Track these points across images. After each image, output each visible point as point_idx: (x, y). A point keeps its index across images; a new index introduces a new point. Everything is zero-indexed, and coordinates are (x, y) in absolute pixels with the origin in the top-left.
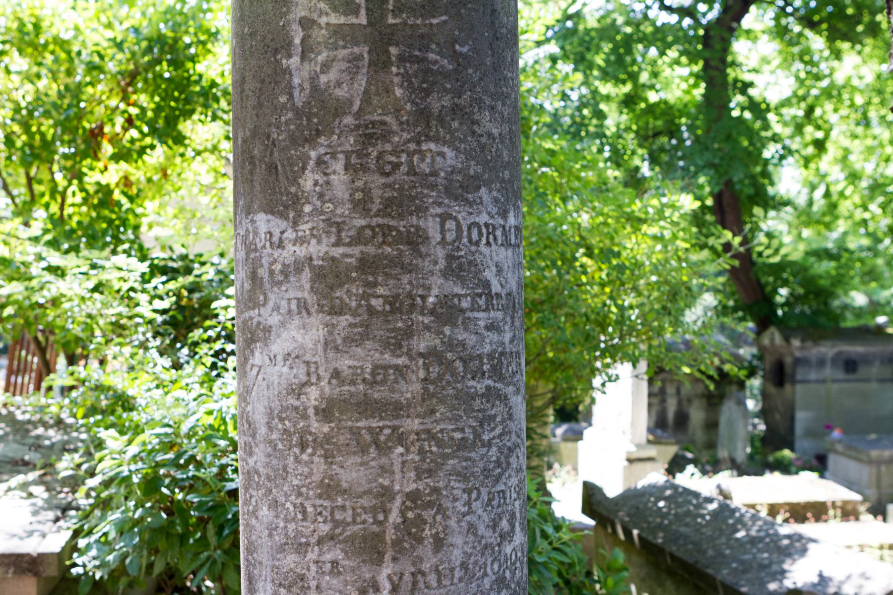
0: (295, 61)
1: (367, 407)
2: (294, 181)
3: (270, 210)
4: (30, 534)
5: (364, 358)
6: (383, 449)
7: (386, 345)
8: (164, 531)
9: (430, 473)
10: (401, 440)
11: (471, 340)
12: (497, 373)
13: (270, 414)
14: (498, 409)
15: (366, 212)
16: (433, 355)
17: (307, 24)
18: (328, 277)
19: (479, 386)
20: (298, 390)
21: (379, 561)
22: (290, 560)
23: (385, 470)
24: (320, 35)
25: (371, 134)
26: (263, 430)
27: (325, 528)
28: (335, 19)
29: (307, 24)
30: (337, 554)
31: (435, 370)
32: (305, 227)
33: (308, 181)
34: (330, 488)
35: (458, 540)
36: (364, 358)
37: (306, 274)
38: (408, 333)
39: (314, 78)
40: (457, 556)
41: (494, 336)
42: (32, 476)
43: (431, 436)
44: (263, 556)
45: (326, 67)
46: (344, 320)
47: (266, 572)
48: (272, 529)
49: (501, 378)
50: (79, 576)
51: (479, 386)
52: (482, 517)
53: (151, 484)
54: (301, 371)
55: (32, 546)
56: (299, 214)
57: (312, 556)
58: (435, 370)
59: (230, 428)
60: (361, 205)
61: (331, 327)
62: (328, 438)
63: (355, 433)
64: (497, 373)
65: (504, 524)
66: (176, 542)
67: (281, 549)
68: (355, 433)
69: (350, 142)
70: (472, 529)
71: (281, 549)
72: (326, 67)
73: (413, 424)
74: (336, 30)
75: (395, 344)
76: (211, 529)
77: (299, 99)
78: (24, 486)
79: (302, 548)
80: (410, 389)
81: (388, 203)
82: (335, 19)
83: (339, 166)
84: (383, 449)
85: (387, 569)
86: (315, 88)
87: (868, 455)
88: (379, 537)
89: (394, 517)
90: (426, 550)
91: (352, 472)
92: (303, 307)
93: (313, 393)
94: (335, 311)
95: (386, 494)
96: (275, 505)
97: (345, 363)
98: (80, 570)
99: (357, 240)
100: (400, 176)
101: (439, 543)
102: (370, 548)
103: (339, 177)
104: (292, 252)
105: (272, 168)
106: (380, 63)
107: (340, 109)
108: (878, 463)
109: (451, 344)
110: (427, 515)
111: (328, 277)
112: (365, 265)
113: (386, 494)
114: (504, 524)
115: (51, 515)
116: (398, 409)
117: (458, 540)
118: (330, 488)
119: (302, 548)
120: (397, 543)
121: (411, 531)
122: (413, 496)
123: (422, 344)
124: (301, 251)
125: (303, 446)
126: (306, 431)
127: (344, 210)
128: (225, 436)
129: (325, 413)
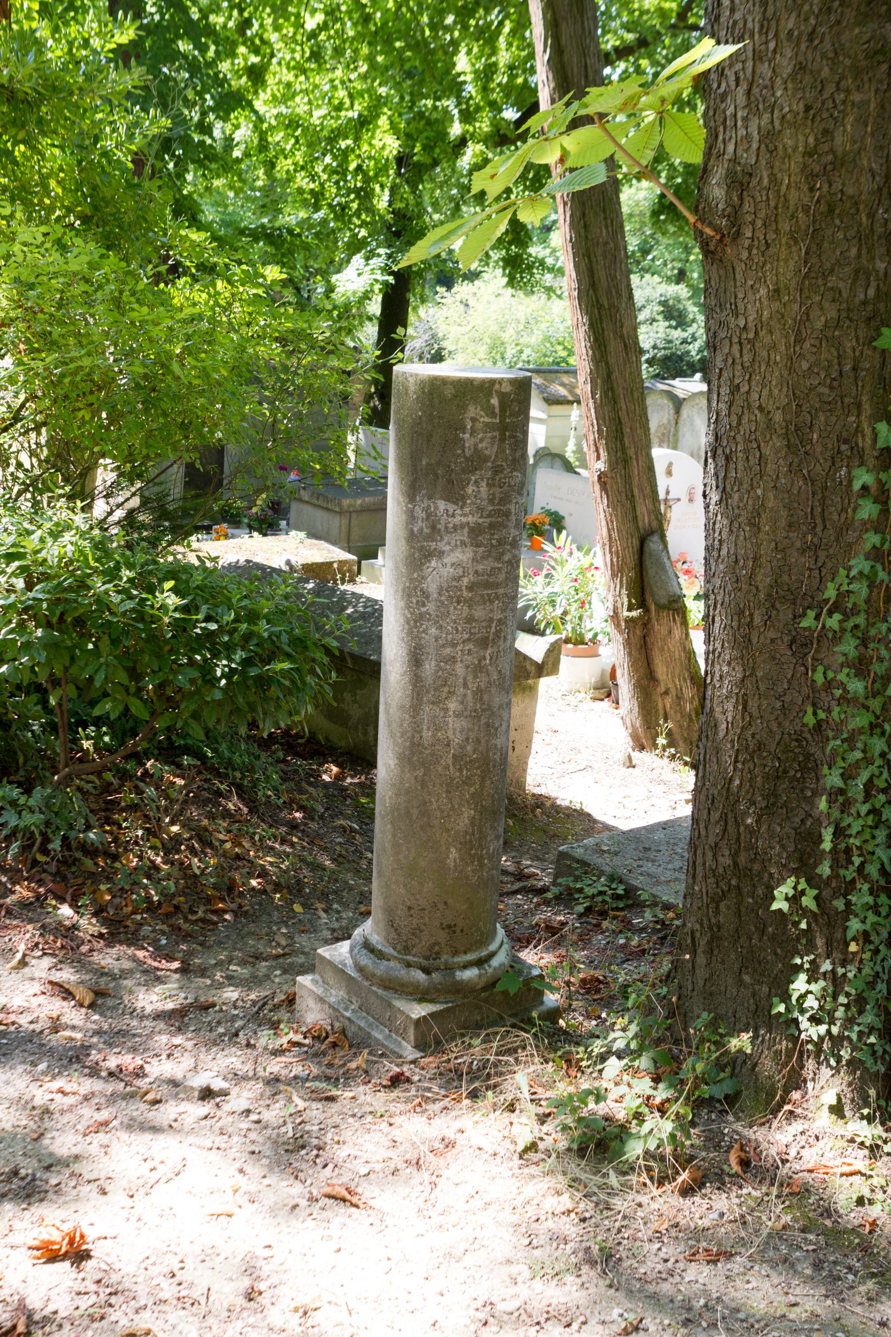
0: (467, 436)
1: (487, 585)
2: (463, 489)
3: (448, 499)
13: (441, 589)
15: (493, 504)
17: (474, 420)
18: (475, 531)
20: (458, 579)
24: (479, 426)
25: (497, 470)
27: (466, 636)
28: (487, 420)
29: (474, 420)
32: (467, 510)
33: (470, 490)
34: (470, 620)
37: (466, 530)
38: (503, 554)
39: (476, 445)
45: (481, 440)
46: (482, 549)
56: (464, 504)
60: (491, 501)
61: (476, 552)
63: (482, 596)
69: (489, 474)
72: (481, 440)
73: (501, 591)
74: (487, 425)
75: (498, 559)
77: (468, 453)
79: (454, 645)
81: (501, 499)
82: (487, 420)
83: (484, 484)
86: (476, 449)
87: (339, 504)
90: (501, 642)
91: (479, 612)
92: (463, 544)
93: (465, 581)
94: (477, 546)
97: (480, 567)
99: (488, 516)
100: (506, 488)
103: (484, 488)
104: (458, 519)
105: (450, 482)
106: (502, 440)
107: (486, 459)
108: (350, 513)
111: (475, 531)
112: (492, 526)
113: (491, 620)
116: (497, 585)
119: (454, 645)
122: (499, 620)
124: (464, 520)
125: (459, 602)
127: (485, 503)
129: (470, 588)
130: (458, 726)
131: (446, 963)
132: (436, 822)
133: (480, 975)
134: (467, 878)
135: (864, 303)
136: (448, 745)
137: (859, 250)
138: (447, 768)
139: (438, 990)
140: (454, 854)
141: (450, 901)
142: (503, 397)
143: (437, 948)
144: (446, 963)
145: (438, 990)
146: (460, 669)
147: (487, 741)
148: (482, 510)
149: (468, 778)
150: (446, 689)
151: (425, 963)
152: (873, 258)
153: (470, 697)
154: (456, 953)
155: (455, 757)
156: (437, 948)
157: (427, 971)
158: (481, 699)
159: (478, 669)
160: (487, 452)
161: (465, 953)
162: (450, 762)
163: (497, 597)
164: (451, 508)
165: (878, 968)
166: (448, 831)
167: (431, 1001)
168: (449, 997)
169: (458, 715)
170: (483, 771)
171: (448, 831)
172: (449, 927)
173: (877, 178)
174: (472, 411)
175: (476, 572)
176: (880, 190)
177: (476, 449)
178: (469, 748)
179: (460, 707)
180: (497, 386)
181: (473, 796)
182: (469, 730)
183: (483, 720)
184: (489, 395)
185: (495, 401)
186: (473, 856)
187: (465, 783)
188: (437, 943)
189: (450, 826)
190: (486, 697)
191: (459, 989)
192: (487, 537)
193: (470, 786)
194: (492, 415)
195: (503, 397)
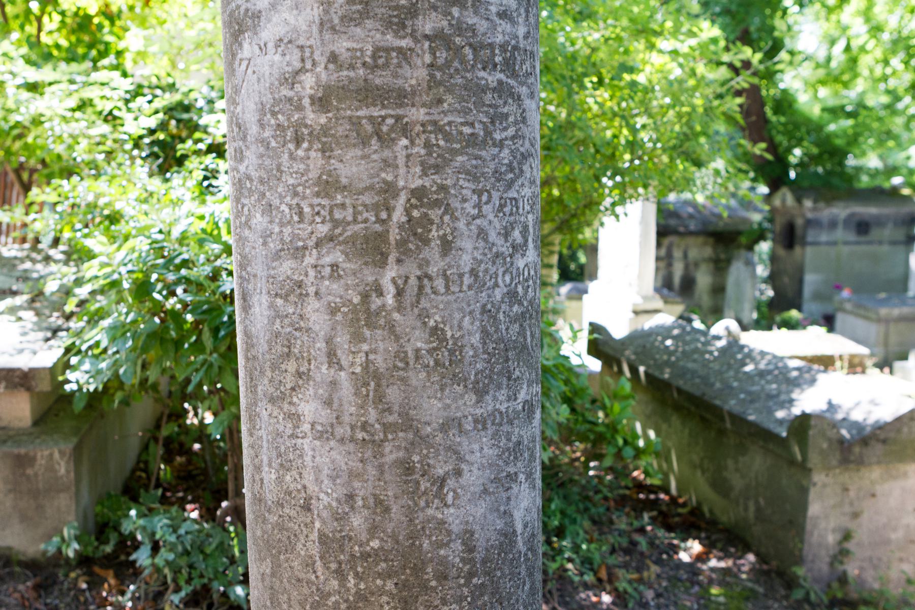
1: (368, 94)
4: (21, 351)
5: (365, 38)
6: (386, 141)
7: (388, 24)
8: (157, 337)
9: (437, 169)
10: (405, 130)
11: (482, 26)
12: (509, 66)
13: (262, 111)
14: (510, 108)
16: (438, 38)
19: (492, 78)
20: (291, 79)
21: (382, 263)
22: (286, 267)
23: (387, 164)
26: (254, 129)
27: (323, 229)
30: (337, 256)
31: (442, 55)
34: (328, 185)
35: (468, 245)
36: (365, 38)
40: (466, 261)
41: (505, 26)
42: (19, 300)
43: (438, 129)
44: (258, 268)
47: (261, 284)
48: (266, 236)
49: (514, 75)
50: (73, 393)
51: (492, 78)
52: (494, 225)
53: (142, 289)
54: (294, 58)
55: (24, 362)
57: (309, 260)
58: (442, 55)
59: (224, 232)
62: (325, 130)
63: (355, 123)
64: (509, 66)
65: (516, 234)
66: (171, 347)
67: (277, 256)
68: (355, 123)
70: (482, 234)
71: (277, 256)
76: (207, 336)
78: (12, 310)
79: (299, 253)
80: (415, 75)
84: (386, 141)
85: (391, 272)
87: (877, 314)
88: (382, 237)
89: (398, 215)
90: (433, 252)
91: (352, 166)
93: (308, 80)
95: (390, 190)
96: (269, 208)
97: (342, 45)
98: (74, 387)
101: (447, 246)
102: (373, 249)
108: (887, 321)
109: (460, 28)
110: (435, 214)
113: (390, 190)
114: (516, 234)
115: (41, 335)
116: (402, 97)
117: (468, 245)
118: (328, 185)
119: (299, 253)
120: (401, 244)
121: (417, 230)
122: (419, 193)
123: (428, 24)
125: (298, 142)
126: (302, 123)
128: (217, 239)
129: (321, 102)
130: (323, 460)
136: (307, 508)
138: (309, 564)
146: (316, 316)
147: (410, 513)
150: (291, 366)
155: (323, 539)
158: (380, 398)
159: (364, 316)
162: (315, 550)
169: (324, 434)
170: (402, 586)
175: (333, 58)
178: (357, 521)
182: (353, 475)
183: (391, 454)
190: (393, 394)
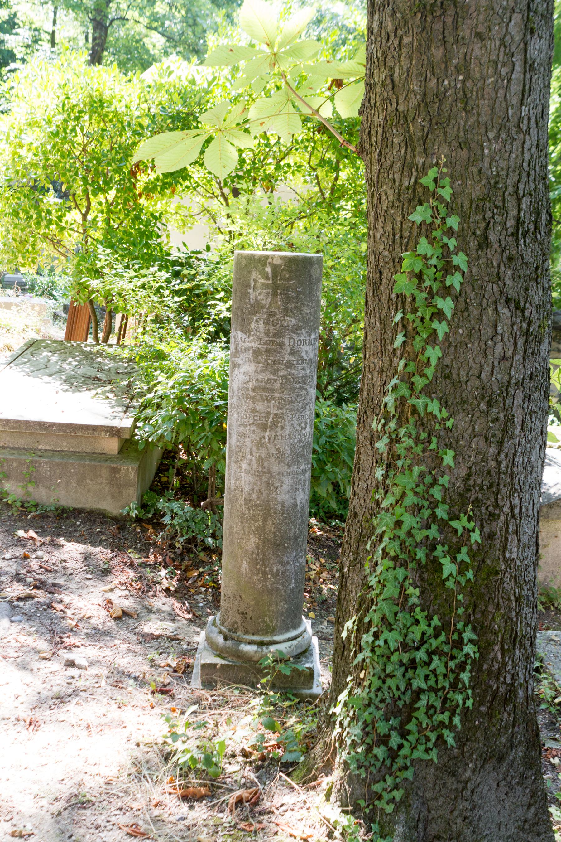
0: (251, 291)
1: (265, 389)
2: (249, 325)
3: (242, 331)
4: (115, 417)
5: (266, 376)
6: (269, 401)
7: (271, 373)
8: (184, 422)
9: (281, 409)
10: (274, 399)
11: (296, 373)
12: (304, 382)
14: (303, 392)
15: (268, 336)
16: (284, 377)
17: (255, 281)
18: (257, 353)
19: (298, 386)
20: (247, 383)
21: (266, 431)
22: (242, 429)
23: (269, 407)
24: (259, 285)
25: (271, 314)
26: (236, 393)
27: (252, 421)
28: (263, 281)
29: (255, 281)
30: (254, 428)
31: (284, 381)
32: (251, 338)
33: (253, 325)
34: (254, 410)
35: (288, 428)
36: (266, 376)
37: (251, 351)
38: (278, 370)
39: (256, 297)
40: (287, 432)
41: (303, 372)
42: (108, 388)
43: (282, 399)
44: (234, 427)
45: (260, 294)
46: (261, 365)
47: (235, 432)
48: (237, 420)
49: (305, 383)
50: (138, 440)
51: (298, 386)
52: (296, 422)
53: (180, 400)
54: (248, 378)
55: (116, 423)
56: (250, 335)
57: (248, 428)
58: (284, 381)
59: (217, 376)
60: (267, 334)
61: (257, 367)
62: (254, 397)
63: (262, 396)
64: (304, 382)
65: (303, 425)
66: (190, 427)
67: (239, 426)
68: (262, 396)
69: (265, 316)
70: (292, 425)
71: (239, 426)
72: (260, 294)
73: (277, 395)
74: (263, 284)
75: (274, 373)
76: (207, 423)
77: (252, 302)
78: (104, 393)
79: (245, 426)
80: (277, 385)
81: (274, 334)
82: (263, 281)
83: (261, 322)
84: (269, 401)
85: (268, 433)
86: (256, 300)
88: (266, 425)
89: (271, 420)
90: (279, 429)
91: (260, 407)
92: (249, 360)
94: (258, 362)
95: (269, 413)
96: (238, 413)
97: (260, 377)
98: (139, 438)
99: (266, 344)
100: (278, 327)
101: (282, 428)
102: (264, 427)
103: (261, 326)
104: (247, 345)
105: (243, 320)
106: (275, 295)
107: (263, 307)
109: (290, 374)
110: (280, 420)
111: (257, 353)
112: (267, 351)
113: (269, 413)
114: (303, 425)
115: (120, 409)
116: (273, 391)
117: (288, 428)
118: (254, 410)
119: (245, 426)
120: (271, 427)
121: (275, 424)
122: (276, 415)
123: (281, 373)
124: (250, 345)
126: (248, 394)
127: (262, 335)
128: (214, 380)
129: (254, 390)
130: (247, 479)
131: (238, 637)
132: (236, 541)
133: (256, 652)
134: (254, 583)
135: (408, 188)
136: (242, 491)
137: (406, 150)
138: (241, 506)
139: (227, 652)
140: (245, 565)
141: (243, 596)
142: (275, 268)
143: (236, 626)
144: (238, 637)
145: (227, 652)
146: (248, 442)
147: (268, 495)
148: (261, 339)
149: (253, 516)
150: (241, 454)
151: (227, 633)
152: (415, 156)
153: (254, 462)
154: (246, 632)
155: (245, 500)
156: (236, 626)
157: (226, 639)
158: (262, 465)
159: (260, 444)
160: (263, 302)
161: (253, 634)
162: (243, 502)
163: (274, 399)
164: (244, 336)
165: (372, 695)
166: (242, 548)
167: (223, 658)
168: (235, 660)
169: (247, 473)
170: (264, 514)
171: (242, 548)
172: (242, 613)
173: (418, 97)
174: (255, 275)
175: (257, 380)
176: (419, 105)
177: (256, 300)
178: (254, 496)
179: (248, 468)
180: (270, 260)
181: (257, 528)
182: (254, 484)
183: (264, 479)
184: (264, 265)
185: (268, 269)
186: (259, 569)
187: (251, 518)
188: (235, 623)
189: (243, 545)
190: (266, 464)
191: (240, 655)
192: (264, 357)
193: (256, 521)
194: (267, 278)
195: (275, 268)
